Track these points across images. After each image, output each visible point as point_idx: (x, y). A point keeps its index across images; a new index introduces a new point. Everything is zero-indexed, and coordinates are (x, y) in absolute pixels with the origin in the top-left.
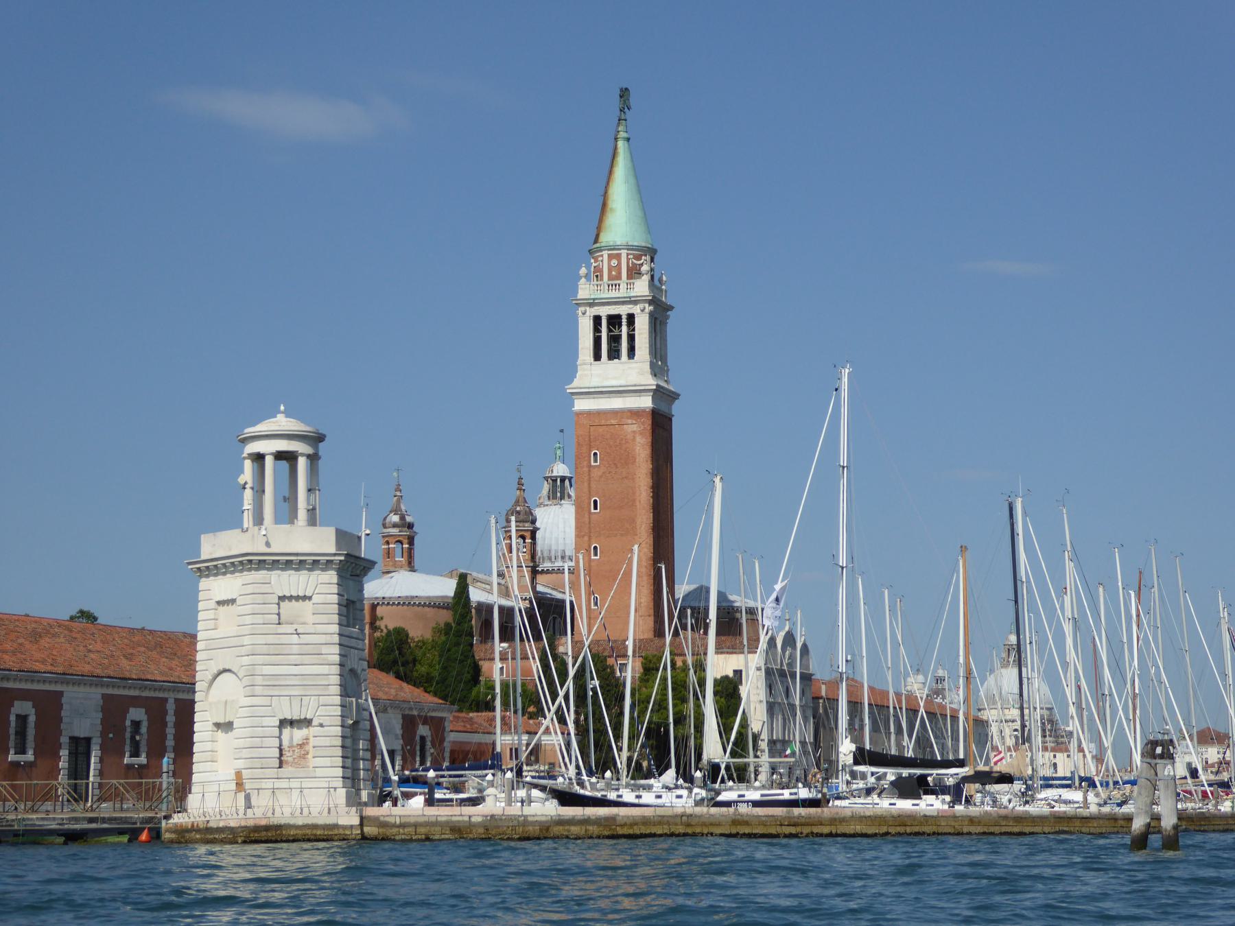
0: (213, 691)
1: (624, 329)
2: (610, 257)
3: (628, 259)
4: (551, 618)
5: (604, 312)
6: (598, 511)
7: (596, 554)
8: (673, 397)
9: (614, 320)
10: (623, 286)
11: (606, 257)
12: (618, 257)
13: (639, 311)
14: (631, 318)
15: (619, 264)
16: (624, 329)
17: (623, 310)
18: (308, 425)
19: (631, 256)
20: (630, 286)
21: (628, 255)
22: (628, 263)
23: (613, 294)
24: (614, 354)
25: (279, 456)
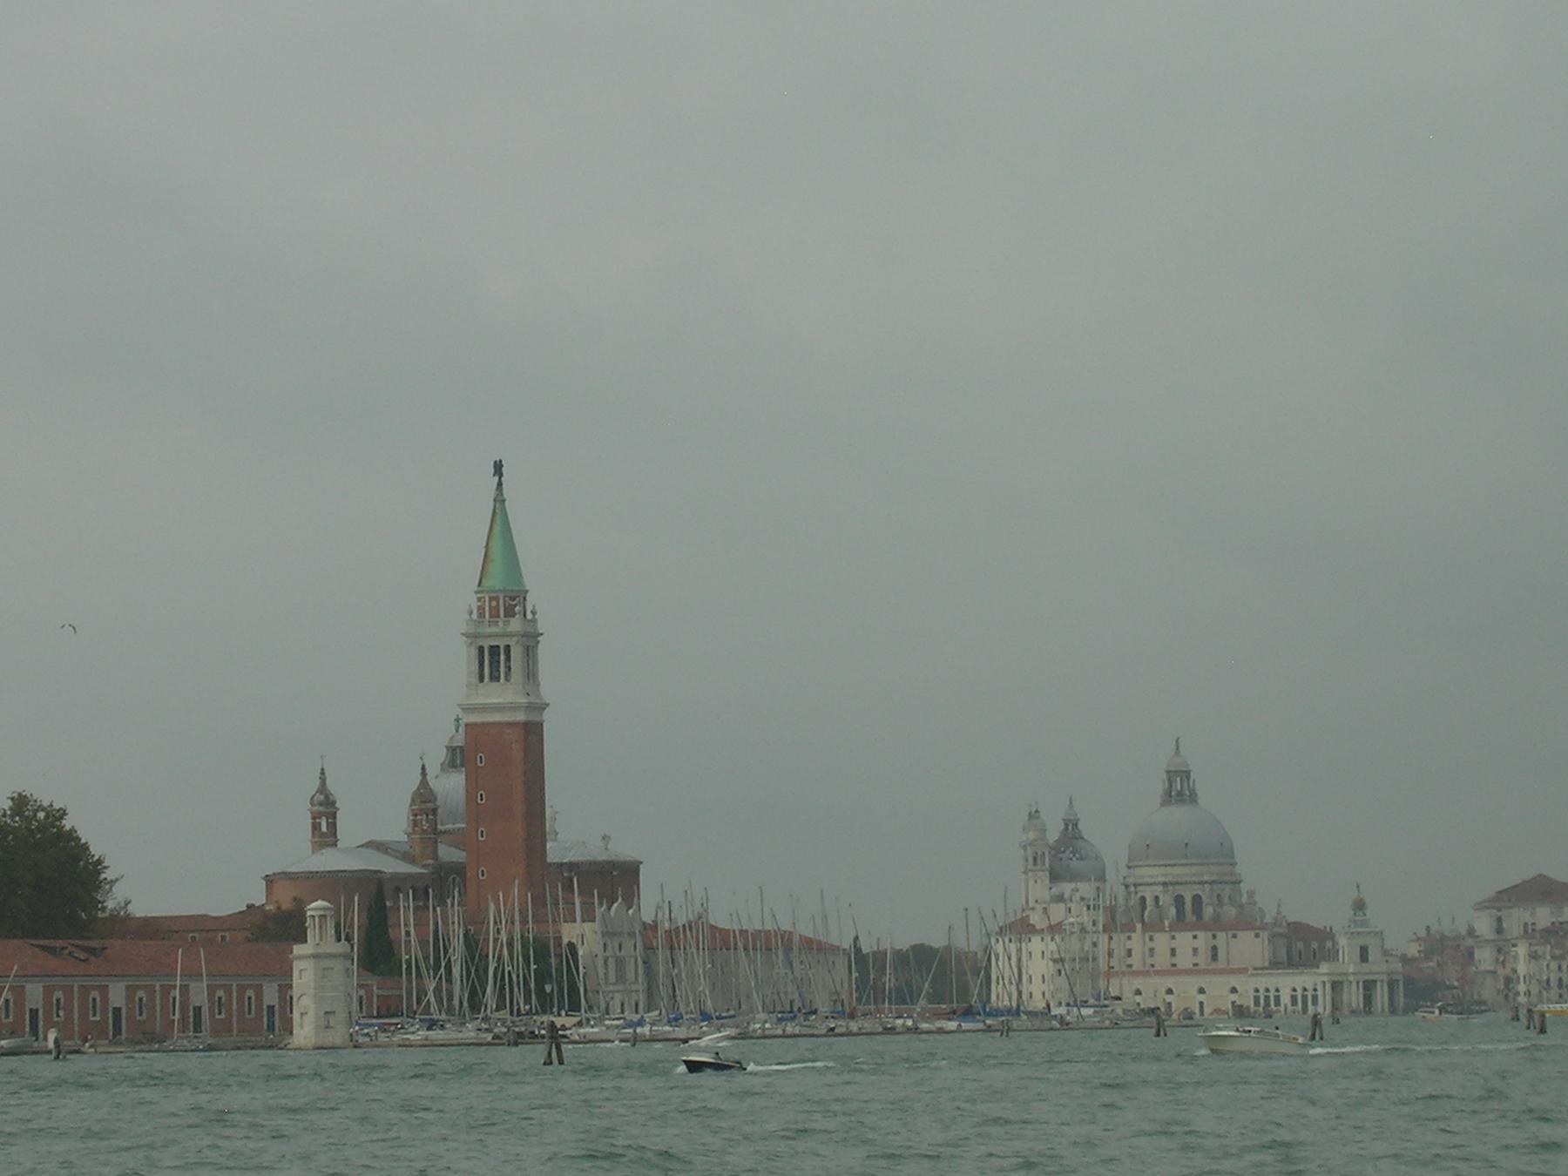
0: (300, 1002)
1: (502, 657)
2: (491, 599)
3: (505, 601)
4: (451, 879)
5: (486, 644)
6: (484, 801)
7: (482, 836)
8: (543, 707)
9: (494, 650)
10: (501, 624)
11: (487, 599)
12: (497, 599)
13: (514, 643)
14: (508, 648)
15: (498, 603)
16: (502, 657)
17: (501, 643)
18: (332, 904)
19: (507, 599)
20: (506, 623)
21: (504, 597)
22: (505, 605)
23: (494, 630)
24: (495, 678)
25: (321, 916)
